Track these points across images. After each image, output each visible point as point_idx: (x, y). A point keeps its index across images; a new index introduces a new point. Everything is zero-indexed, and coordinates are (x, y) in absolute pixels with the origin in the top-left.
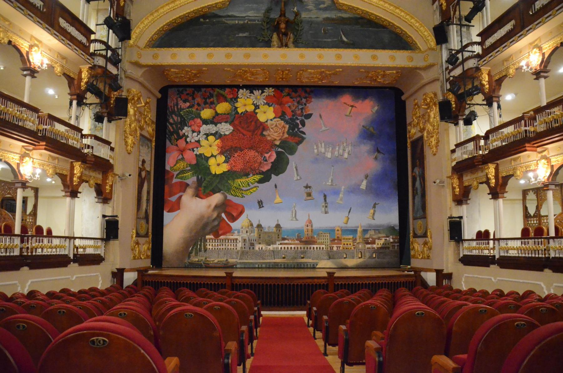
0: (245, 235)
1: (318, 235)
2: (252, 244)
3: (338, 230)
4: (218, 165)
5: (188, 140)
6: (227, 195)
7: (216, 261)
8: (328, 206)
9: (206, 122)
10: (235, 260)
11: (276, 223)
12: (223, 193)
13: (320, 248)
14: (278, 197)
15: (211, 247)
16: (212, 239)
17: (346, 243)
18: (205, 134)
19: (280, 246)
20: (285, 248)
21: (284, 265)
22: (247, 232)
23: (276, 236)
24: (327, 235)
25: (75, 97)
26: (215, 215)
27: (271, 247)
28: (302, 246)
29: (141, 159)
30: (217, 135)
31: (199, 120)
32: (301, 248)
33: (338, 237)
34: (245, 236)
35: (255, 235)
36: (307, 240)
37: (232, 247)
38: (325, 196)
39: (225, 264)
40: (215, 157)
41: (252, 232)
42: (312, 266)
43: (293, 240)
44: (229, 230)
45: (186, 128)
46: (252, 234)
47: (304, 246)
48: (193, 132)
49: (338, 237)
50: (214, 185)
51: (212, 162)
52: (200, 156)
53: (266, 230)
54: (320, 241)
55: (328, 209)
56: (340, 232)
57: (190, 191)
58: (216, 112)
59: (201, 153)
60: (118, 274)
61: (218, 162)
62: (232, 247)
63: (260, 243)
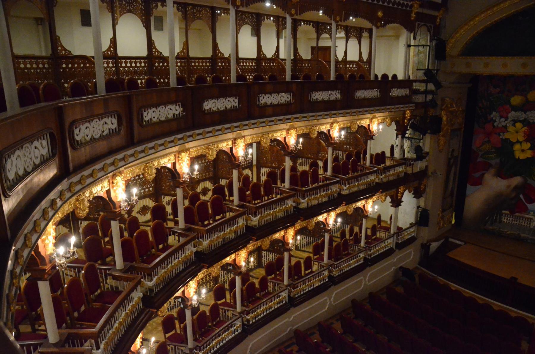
4: (523, 151)
5: (495, 124)
6: (528, 179)
7: (508, 233)
9: (515, 109)
10: (525, 235)
15: (505, 221)
16: (508, 214)
18: (513, 120)
25: (400, 133)
26: (514, 195)
29: (451, 150)
30: (525, 122)
31: (508, 106)
37: (526, 225)
40: (521, 143)
44: (525, 210)
45: (494, 113)
48: (501, 117)
51: (517, 147)
52: (507, 140)
57: (492, 171)
58: (527, 99)
59: (507, 137)
60: (425, 247)
61: (523, 148)
62: (526, 225)
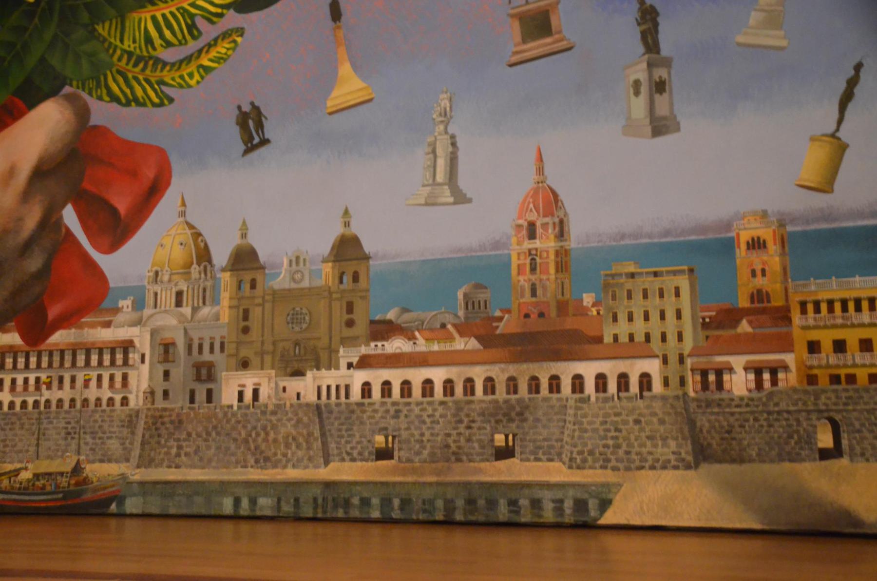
0: (173, 322)
1: (609, 287)
2: (205, 373)
3: (757, 244)
6: (92, 103)
7: (25, 475)
8: (676, 83)
11: (336, 231)
12: (71, 99)
13: (623, 380)
14: (346, 69)
16: (13, 351)
17: (826, 338)
19: (359, 377)
20: (386, 386)
21: (386, 502)
22: (179, 304)
23: (339, 315)
24: (669, 283)
27: (306, 386)
28: (500, 373)
32: (490, 385)
33: (759, 296)
34: (169, 321)
35: (222, 311)
36: (535, 325)
37: (106, 394)
38: (649, 18)
39: (67, 495)
41: (206, 297)
42: (569, 516)
43: (440, 332)
44: (92, 296)
46: (206, 311)
47: (512, 370)
49: (759, 296)
50: (31, 61)
53: (281, 281)
54: (623, 328)
55: (681, 103)
56: (773, 258)
63: (245, 365)
